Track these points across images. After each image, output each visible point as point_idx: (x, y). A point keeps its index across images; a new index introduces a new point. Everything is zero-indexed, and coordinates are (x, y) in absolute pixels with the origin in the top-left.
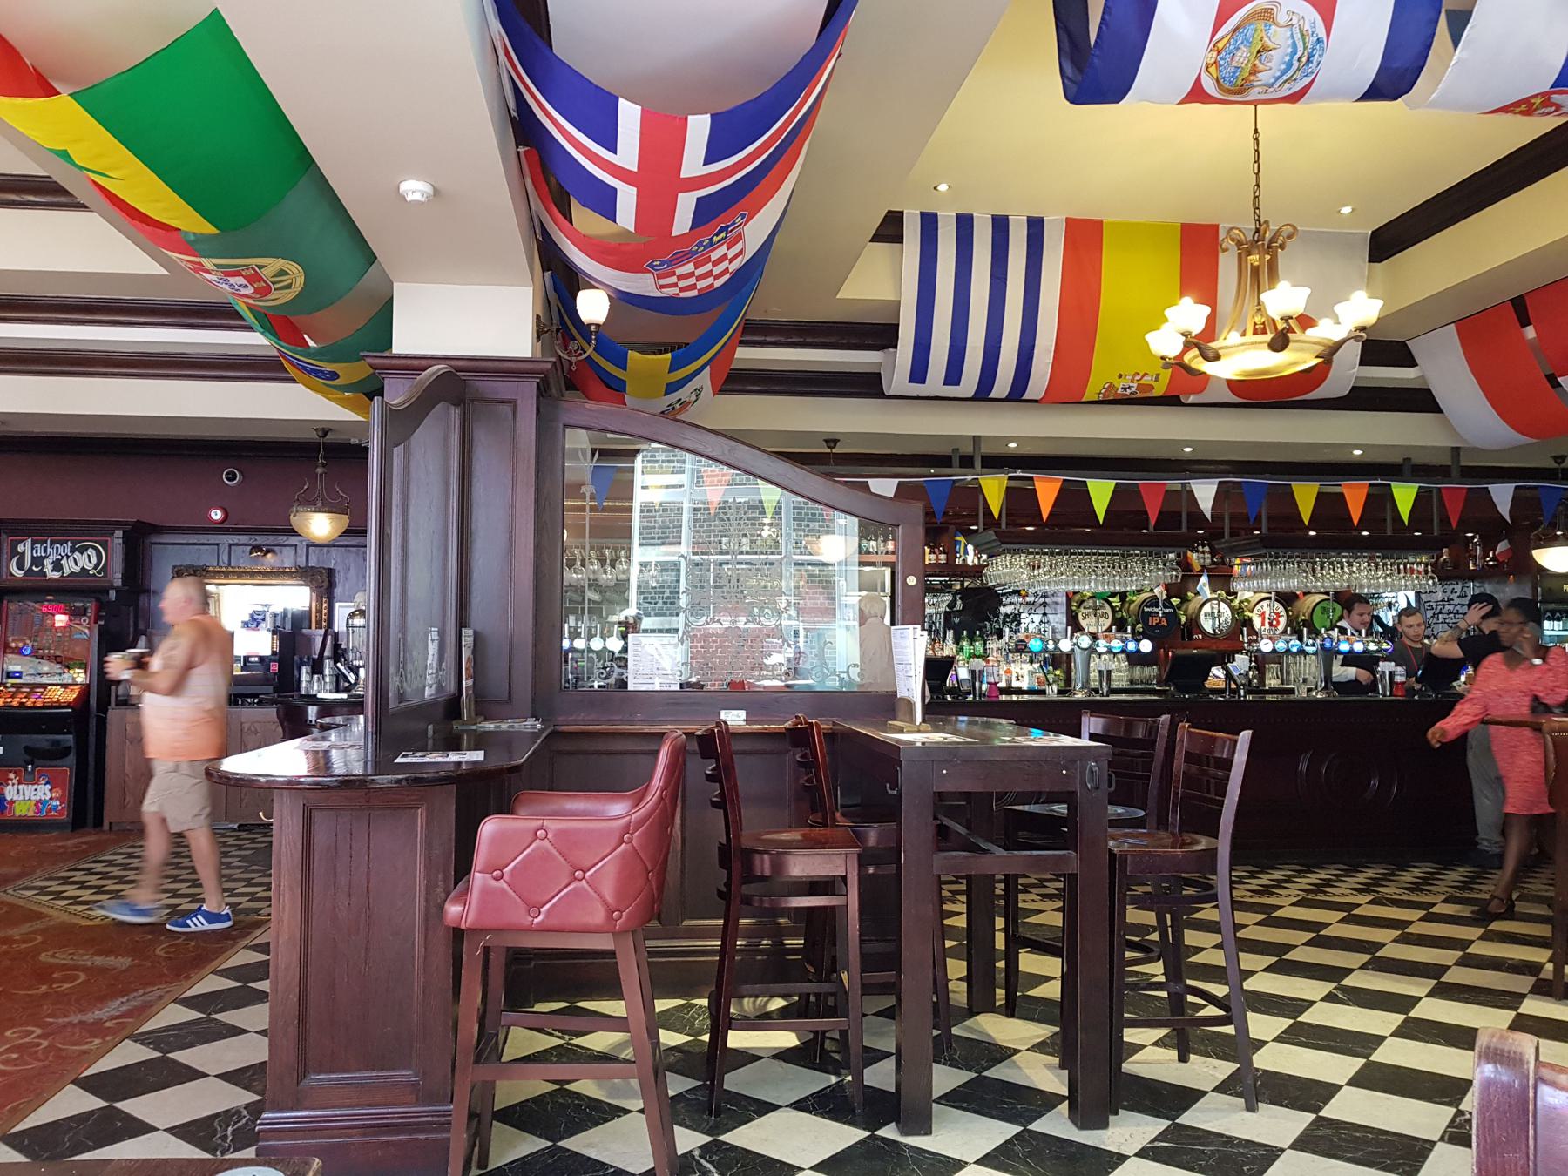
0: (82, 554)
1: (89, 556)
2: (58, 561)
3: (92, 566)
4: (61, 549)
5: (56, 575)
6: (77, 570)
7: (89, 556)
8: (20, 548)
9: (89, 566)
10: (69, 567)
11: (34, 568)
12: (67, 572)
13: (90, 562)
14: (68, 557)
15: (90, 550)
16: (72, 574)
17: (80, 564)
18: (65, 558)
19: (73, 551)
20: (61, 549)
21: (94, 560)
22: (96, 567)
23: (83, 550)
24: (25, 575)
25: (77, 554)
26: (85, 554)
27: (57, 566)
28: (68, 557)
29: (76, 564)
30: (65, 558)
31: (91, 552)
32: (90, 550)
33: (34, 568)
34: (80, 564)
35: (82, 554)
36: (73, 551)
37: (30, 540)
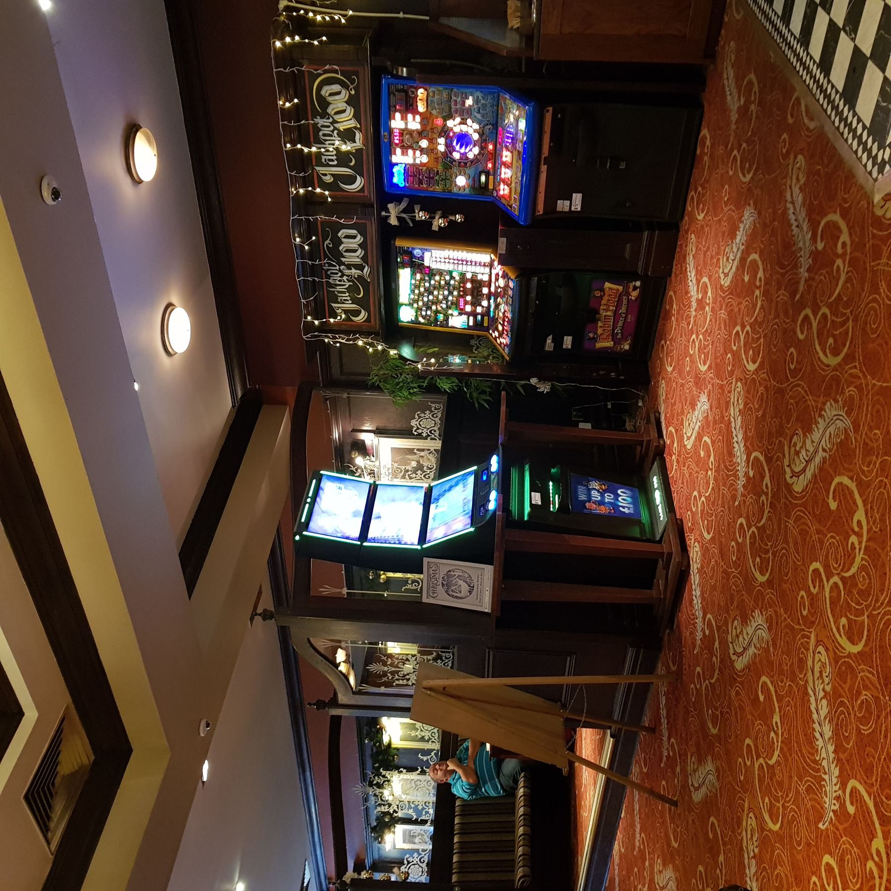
0: (329, 104)
1: (331, 94)
2: (340, 134)
3: (344, 92)
4: (326, 131)
5: (358, 136)
6: (350, 112)
7: (331, 94)
8: (328, 179)
9: (345, 95)
10: (347, 121)
11: (352, 164)
12: (352, 124)
13: (339, 93)
14: (335, 122)
15: (323, 93)
16: (357, 116)
17: (342, 106)
18: (337, 125)
19: (325, 115)
20: (326, 131)
21: (336, 88)
22: (344, 85)
23: (324, 104)
24: (362, 175)
25: (330, 110)
26: (330, 99)
27: (348, 135)
28: (335, 122)
29: (344, 111)
30: (337, 125)
31: (326, 91)
32: (323, 93)
33: (352, 164)
34: (342, 106)
35: (329, 104)
36: (325, 115)
37: (317, 168)
